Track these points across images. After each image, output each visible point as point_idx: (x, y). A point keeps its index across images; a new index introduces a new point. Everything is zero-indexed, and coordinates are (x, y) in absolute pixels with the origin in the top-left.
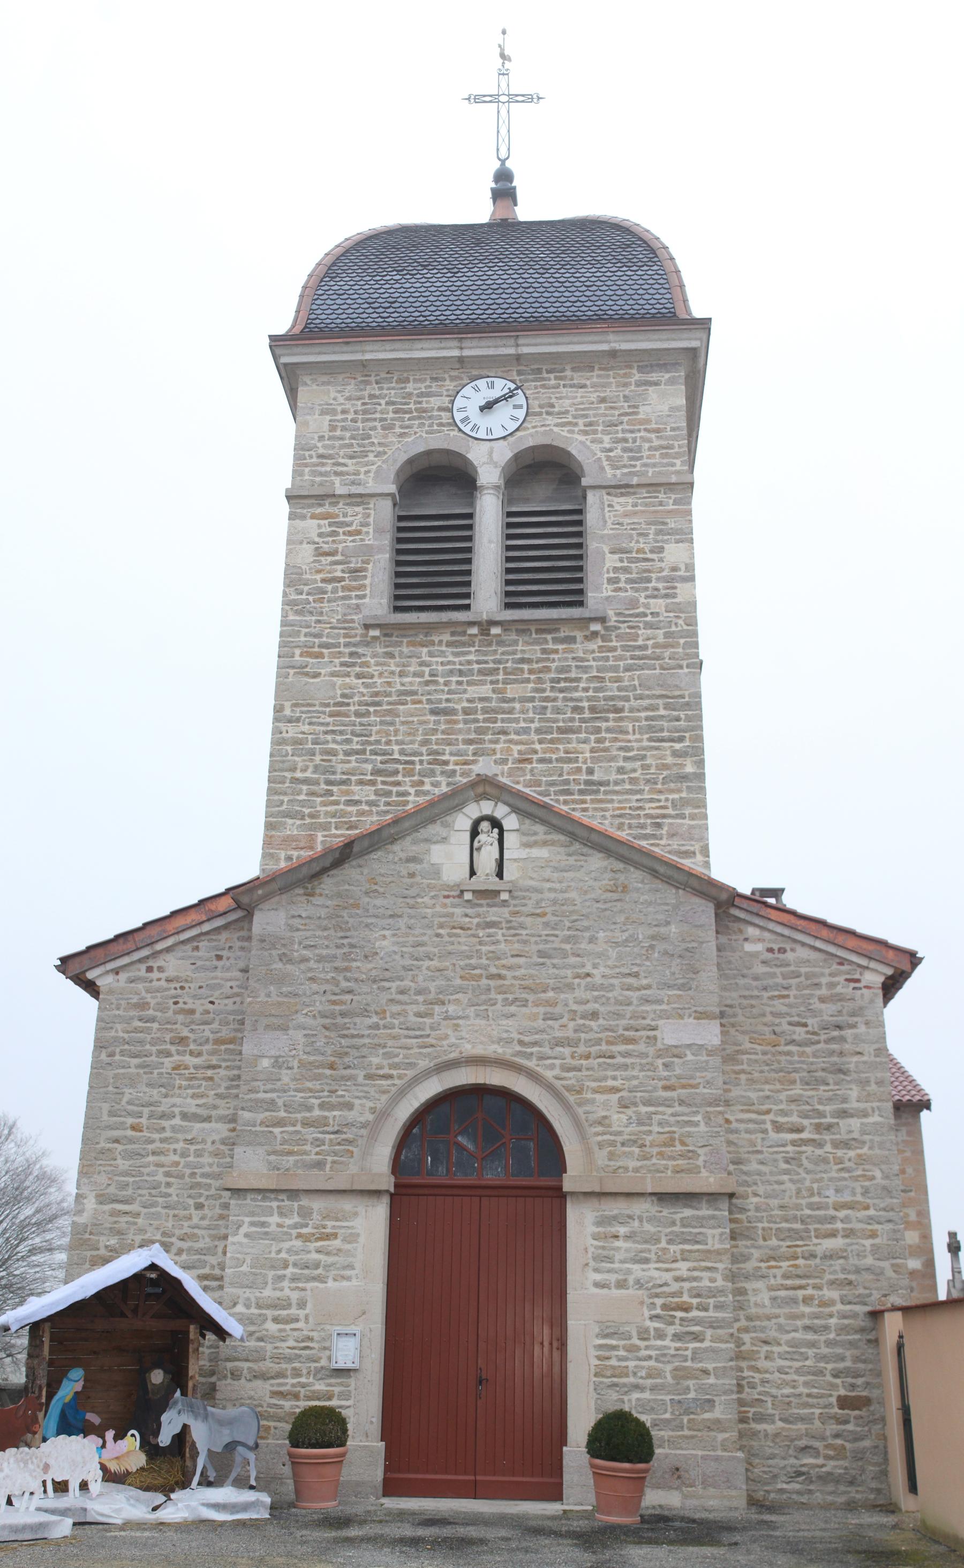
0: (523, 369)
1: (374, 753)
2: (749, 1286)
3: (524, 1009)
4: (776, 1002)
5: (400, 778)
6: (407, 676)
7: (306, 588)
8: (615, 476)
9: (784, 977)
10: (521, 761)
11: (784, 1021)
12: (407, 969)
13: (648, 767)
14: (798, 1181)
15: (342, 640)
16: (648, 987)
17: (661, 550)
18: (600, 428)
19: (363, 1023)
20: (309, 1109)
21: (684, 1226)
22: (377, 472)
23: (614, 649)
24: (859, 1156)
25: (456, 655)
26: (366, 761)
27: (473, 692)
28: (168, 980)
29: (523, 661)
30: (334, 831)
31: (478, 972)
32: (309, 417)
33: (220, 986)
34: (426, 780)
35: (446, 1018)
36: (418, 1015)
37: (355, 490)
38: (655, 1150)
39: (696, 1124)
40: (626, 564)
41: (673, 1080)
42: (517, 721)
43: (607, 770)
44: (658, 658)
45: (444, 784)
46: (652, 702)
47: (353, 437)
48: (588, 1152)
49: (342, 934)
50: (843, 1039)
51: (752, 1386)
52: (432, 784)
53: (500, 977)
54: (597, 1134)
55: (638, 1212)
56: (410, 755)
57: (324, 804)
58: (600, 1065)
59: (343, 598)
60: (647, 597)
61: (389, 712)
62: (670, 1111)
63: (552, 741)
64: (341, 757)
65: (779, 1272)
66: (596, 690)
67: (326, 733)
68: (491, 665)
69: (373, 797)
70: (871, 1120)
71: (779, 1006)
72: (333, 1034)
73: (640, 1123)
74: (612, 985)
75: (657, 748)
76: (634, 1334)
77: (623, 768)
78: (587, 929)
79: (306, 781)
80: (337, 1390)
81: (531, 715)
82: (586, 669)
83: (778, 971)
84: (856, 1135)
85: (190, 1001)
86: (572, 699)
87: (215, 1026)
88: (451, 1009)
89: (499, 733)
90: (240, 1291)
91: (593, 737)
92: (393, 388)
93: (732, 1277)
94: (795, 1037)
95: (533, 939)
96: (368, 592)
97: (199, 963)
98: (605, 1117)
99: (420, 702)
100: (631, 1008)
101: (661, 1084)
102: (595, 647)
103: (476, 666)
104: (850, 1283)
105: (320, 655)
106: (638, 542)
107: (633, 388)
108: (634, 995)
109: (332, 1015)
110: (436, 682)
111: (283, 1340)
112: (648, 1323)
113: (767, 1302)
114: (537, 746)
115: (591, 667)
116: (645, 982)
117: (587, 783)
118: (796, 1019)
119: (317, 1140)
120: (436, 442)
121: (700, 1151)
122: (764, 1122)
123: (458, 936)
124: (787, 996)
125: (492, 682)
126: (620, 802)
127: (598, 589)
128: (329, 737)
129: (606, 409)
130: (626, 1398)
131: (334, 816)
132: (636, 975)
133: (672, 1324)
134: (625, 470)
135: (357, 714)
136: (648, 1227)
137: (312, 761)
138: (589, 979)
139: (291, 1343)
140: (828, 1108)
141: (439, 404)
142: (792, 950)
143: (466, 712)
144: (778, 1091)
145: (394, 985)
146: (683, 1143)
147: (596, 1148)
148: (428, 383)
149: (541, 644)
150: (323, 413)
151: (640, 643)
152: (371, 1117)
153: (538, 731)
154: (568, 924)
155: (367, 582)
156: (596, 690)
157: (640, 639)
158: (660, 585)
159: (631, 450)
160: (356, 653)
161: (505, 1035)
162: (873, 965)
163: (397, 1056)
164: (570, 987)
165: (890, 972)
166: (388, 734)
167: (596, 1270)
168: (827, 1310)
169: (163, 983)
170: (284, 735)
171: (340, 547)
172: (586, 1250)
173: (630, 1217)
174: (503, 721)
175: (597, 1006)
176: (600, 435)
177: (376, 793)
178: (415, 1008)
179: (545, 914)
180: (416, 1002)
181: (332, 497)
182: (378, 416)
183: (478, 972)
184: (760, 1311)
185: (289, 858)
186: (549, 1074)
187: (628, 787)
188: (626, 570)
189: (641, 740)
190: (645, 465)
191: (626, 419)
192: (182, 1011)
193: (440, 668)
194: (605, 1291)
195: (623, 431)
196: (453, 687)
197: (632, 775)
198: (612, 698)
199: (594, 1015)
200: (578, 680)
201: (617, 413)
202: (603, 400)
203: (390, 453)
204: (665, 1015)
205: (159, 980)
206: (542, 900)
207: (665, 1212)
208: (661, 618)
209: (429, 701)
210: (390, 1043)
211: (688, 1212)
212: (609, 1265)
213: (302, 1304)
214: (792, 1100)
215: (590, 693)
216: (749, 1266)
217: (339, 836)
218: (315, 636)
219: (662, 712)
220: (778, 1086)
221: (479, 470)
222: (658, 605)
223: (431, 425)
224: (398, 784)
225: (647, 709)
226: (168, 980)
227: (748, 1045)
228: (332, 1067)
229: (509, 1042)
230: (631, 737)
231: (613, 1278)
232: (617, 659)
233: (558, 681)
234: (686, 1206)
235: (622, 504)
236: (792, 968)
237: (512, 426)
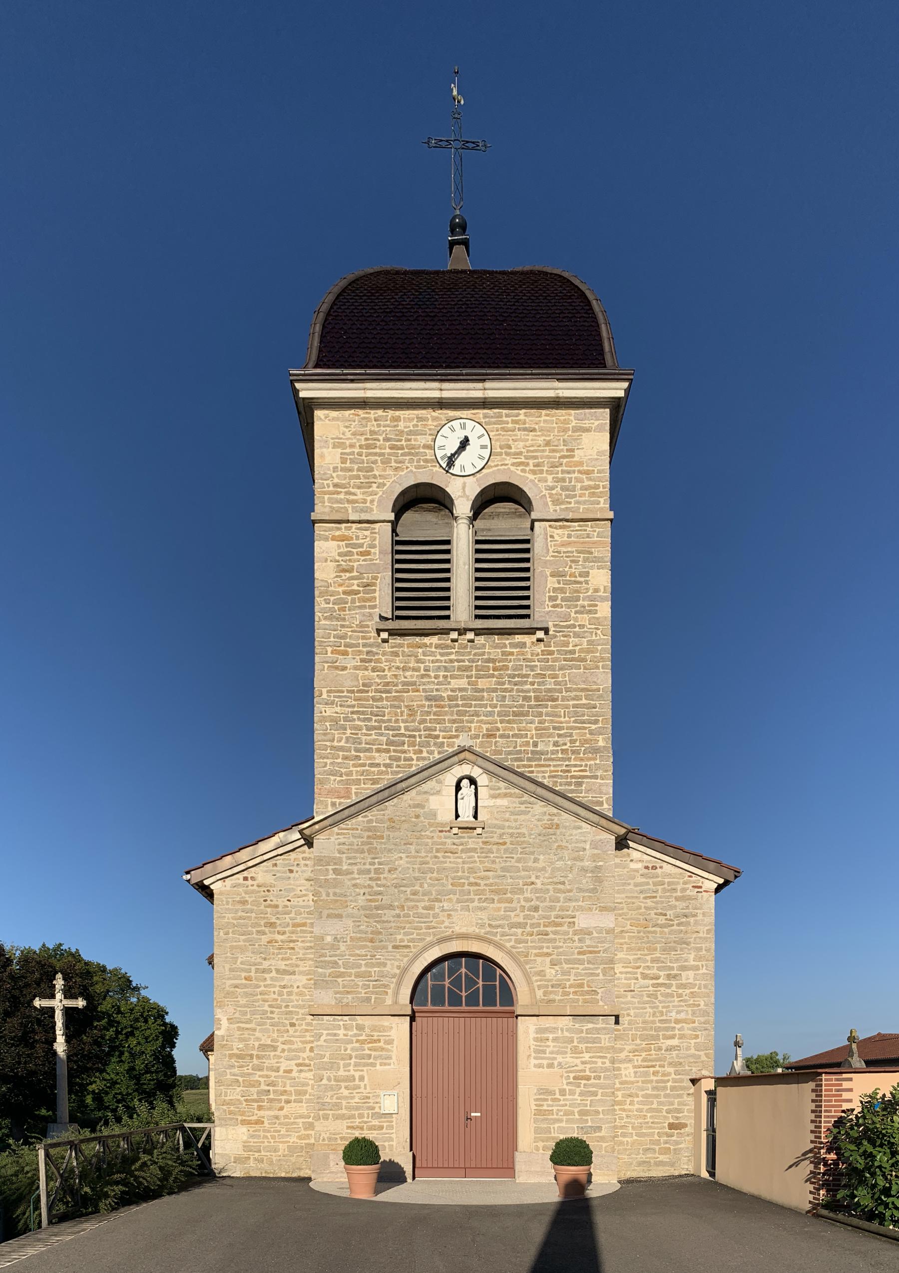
1: (387, 728)
2: (622, 1066)
3: (492, 905)
4: (648, 901)
5: (406, 747)
6: (408, 671)
7: (332, 598)
8: (556, 511)
9: (655, 884)
10: (489, 736)
11: (653, 912)
12: (416, 879)
13: (574, 741)
14: (654, 1007)
15: (360, 641)
16: (570, 891)
17: (587, 574)
18: (545, 469)
19: (388, 915)
20: (360, 966)
21: (587, 1033)
22: (379, 501)
23: (551, 653)
24: (692, 993)
25: (442, 655)
26: (381, 735)
27: (455, 684)
28: (258, 886)
29: (489, 661)
30: (363, 786)
31: (463, 881)
32: (324, 450)
33: (294, 890)
34: (424, 749)
35: (443, 910)
36: (425, 908)
37: (364, 517)
38: (572, 990)
39: (598, 975)
40: (562, 585)
41: (585, 948)
42: (485, 706)
43: (547, 744)
44: (584, 660)
45: (436, 752)
46: (578, 694)
47: (359, 470)
48: (532, 991)
49: (373, 856)
50: (688, 923)
51: (621, 1118)
52: (428, 752)
53: (477, 884)
54: (537, 981)
55: (561, 1026)
56: (413, 731)
57: (354, 766)
58: (539, 939)
59: (360, 607)
60: (576, 613)
61: (396, 698)
62: (581, 967)
63: (509, 722)
64: (364, 731)
65: (640, 1058)
66: (539, 684)
67: (352, 713)
68: (467, 663)
69: (388, 761)
70: (701, 972)
71: (649, 903)
72: (371, 920)
73: (563, 974)
74: (548, 890)
75: (580, 728)
76: (557, 1092)
77: (557, 742)
78: (533, 853)
79: (341, 749)
80: (385, 1124)
81: (495, 702)
82: (532, 668)
83: (651, 881)
84: (691, 981)
85: (274, 899)
86: (522, 691)
87: (292, 915)
88: (446, 905)
89: (473, 716)
90: (324, 1072)
91: (536, 719)
92: (388, 426)
93: (613, 1062)
94: (659, 922)
95: (497, 860)
96: (377, 603)
97: (278, 875)
99: (418, 691)
100: (558, 904)
101: (576, 951)
102: (539, 651)
103: (456, 664)
104: (681, 1064)
105: (345, 653)
106: (571, 567)
107: (570, 433)
108: (562, 896)
109: (370, 908)
110: (429, 676)
111: (353, 1098)
112: (565, 1087)
113: (632, 1075)
114: (499, 725)
115: (536, 666)
116: (568, 887)
117: (532, 752)
118: (660, 911)
119: (365, 985)
121: (599, 991)
122: (636, 973)
123: (449, 857)
124: (655, 897)
125: (468, 677)
126: (554, 766)
127: (542, 604)
128: (355, 716)
129: (550, 451)
131: (362, 775)
132: (563, 883)
133: (579, 1087)
134: (563, 507)
135: (374, 699)
136: (566, 1034)
137: (345, 734)
138: (533, 886)
139: (357, 1100)
140: (675, 965)
141: (424, 442)
142: (661, 867)
143: (450, 698)
144: (646, 955)
145: (409, 890)
146: (589, 986)
148: (415, 422)
149: (502, 648)
150: (334, 447)
151: (571, 648)
152: (398, 972)
153: (499, 714)
154: (520, 850)
155: (377, 594)
156: (539, 684)
157: (571, 645)
158: (586, 603)
159: (568, 490)
160: (371, 652)
161: (480, 921)
162: (711, 877)
163: (413, 934)
164: (521, 891)
165: (721, 881)
166: (396, 715)
167: (535, 1058)
168: (666, 1078)
169: (255, 887)
170: (324, 714)
171: (355, 564)
174: (476, 706)
175: (538, 903)
176: (545, 475)
177: (390, 758)
178: (423, 904)
179: (505, 843)
180: (423, 901)
182: (377, 450)
183: (463, 881)
184: (628, 1079)
185: (334, 804)
186: (508, 945)
187: (560, 755)
188: (562, 590)
189: (569, 722)
190: (578, 502)
191: (565, 461)
192: (270, 906)
193: (431, 665)
195: (563, 472)
196: (441, 679)
197: (564, 747)
198: (550, 690)
199: (536, 909)
200: (527, 676)
201: (558, 455)
202: (548, 444)
203: (388, 484)
204: (581, 908)
205: (252, 885)
206: (503, 834)
207: (577, 1026)
208: (585, 629)
209: (424, 690)
210: (408, 925)
211: (590, 1026)
213: (362, 1078)
214: (653, 961)
215: (536, 686)
216: (623, 1055)
217: (365, 789)
218: (341, 637)
219: (584, 701)
220: (646, 952)
221: (455, 502)
222: (584, 619)
223: (418, 461)
224: (405, 752)
225: (574, 699)
226: (258, 886)
227: (629, 927)
228: (372, 941)
229: (482, 926)
230: (562, 719)
231: (545, 1062)
232: (554, 660)
233: (514, 676)
234: (589, 1022)
235: (560, 534)
236: (659, 879)
237: (480, 464)
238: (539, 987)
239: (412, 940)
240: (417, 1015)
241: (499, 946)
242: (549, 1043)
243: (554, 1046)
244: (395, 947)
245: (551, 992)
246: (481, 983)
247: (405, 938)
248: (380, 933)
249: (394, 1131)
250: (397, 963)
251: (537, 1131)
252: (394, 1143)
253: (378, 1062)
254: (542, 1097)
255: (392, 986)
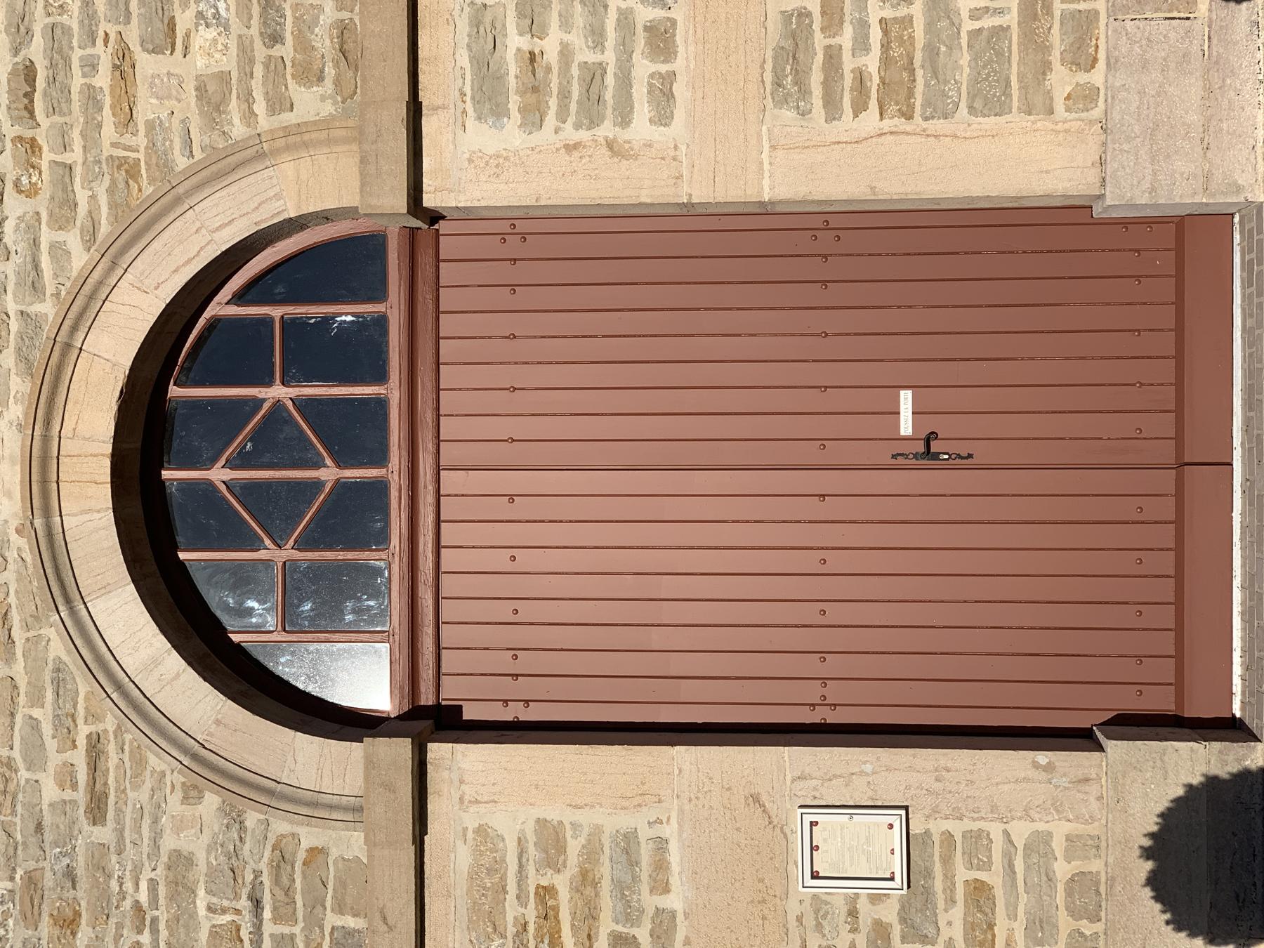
58: (53, 110)
80: (963, 874)
98: (201, 89)
130: (968, 26)
147: (289, 118)
152: (212, 800)
163: (34, 725)
167: (624, 120)
172: (570, 148)
173: (476, 23)
186: (79, 259)
194: (680, 89)
212: (610, 80)
238: (280, 103)
239: (65, 725)
240: (427, 699)
241: (84, 305)
242: (550, 47)
243: (566, 25)
244: (97, 810)
245: (303, 45)
246: (278, 392)
247: (55, 759)
248: (32, 881)
249: (995, 830)
250: (174, 803)
251: (989, 100)
252: (1060, 830)
253: (650, 902)
254: (816, 80)
255: (281, 826)
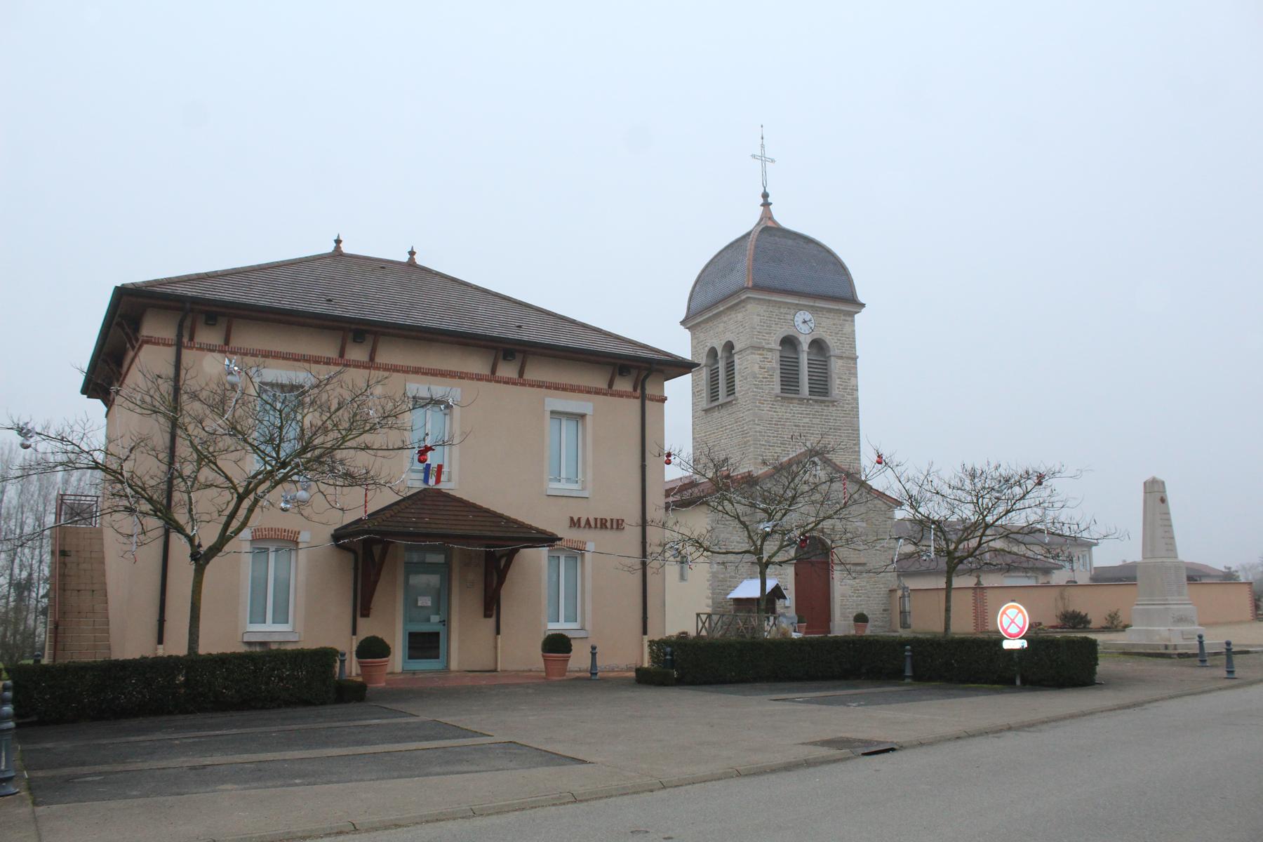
0: (813, 310)
120: (790, 332)
181: (763, 348)
235: (840, 362)
